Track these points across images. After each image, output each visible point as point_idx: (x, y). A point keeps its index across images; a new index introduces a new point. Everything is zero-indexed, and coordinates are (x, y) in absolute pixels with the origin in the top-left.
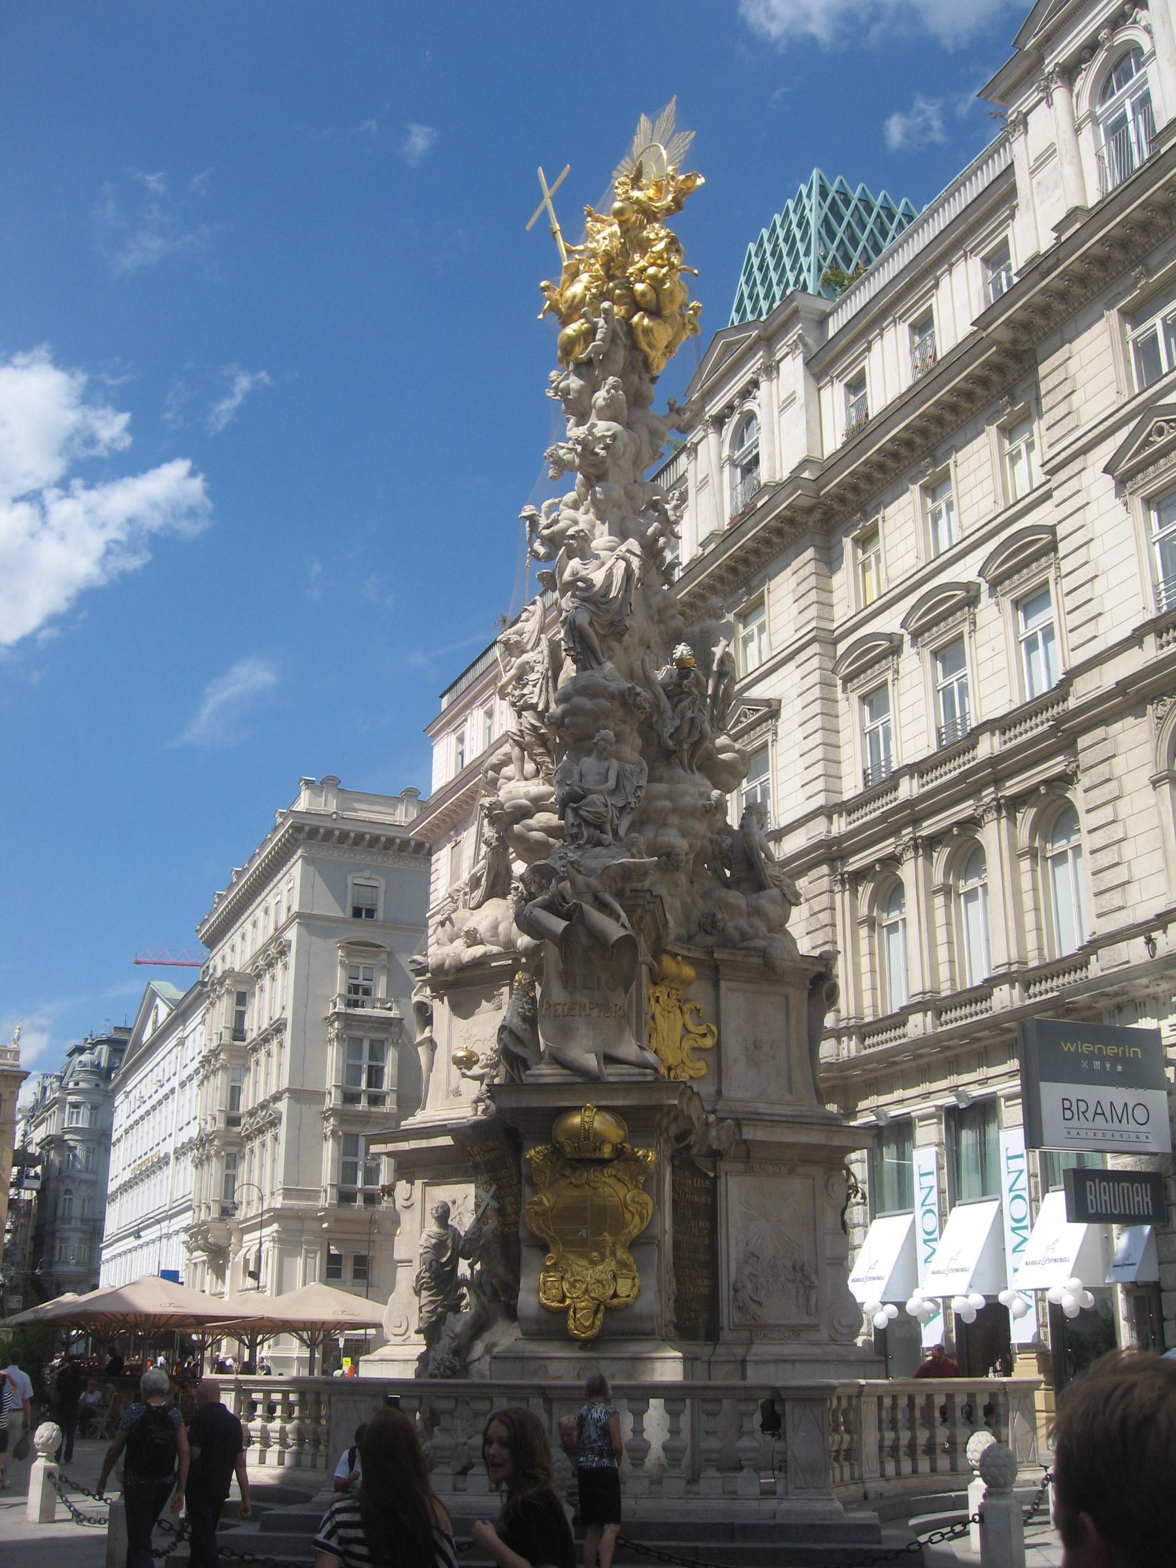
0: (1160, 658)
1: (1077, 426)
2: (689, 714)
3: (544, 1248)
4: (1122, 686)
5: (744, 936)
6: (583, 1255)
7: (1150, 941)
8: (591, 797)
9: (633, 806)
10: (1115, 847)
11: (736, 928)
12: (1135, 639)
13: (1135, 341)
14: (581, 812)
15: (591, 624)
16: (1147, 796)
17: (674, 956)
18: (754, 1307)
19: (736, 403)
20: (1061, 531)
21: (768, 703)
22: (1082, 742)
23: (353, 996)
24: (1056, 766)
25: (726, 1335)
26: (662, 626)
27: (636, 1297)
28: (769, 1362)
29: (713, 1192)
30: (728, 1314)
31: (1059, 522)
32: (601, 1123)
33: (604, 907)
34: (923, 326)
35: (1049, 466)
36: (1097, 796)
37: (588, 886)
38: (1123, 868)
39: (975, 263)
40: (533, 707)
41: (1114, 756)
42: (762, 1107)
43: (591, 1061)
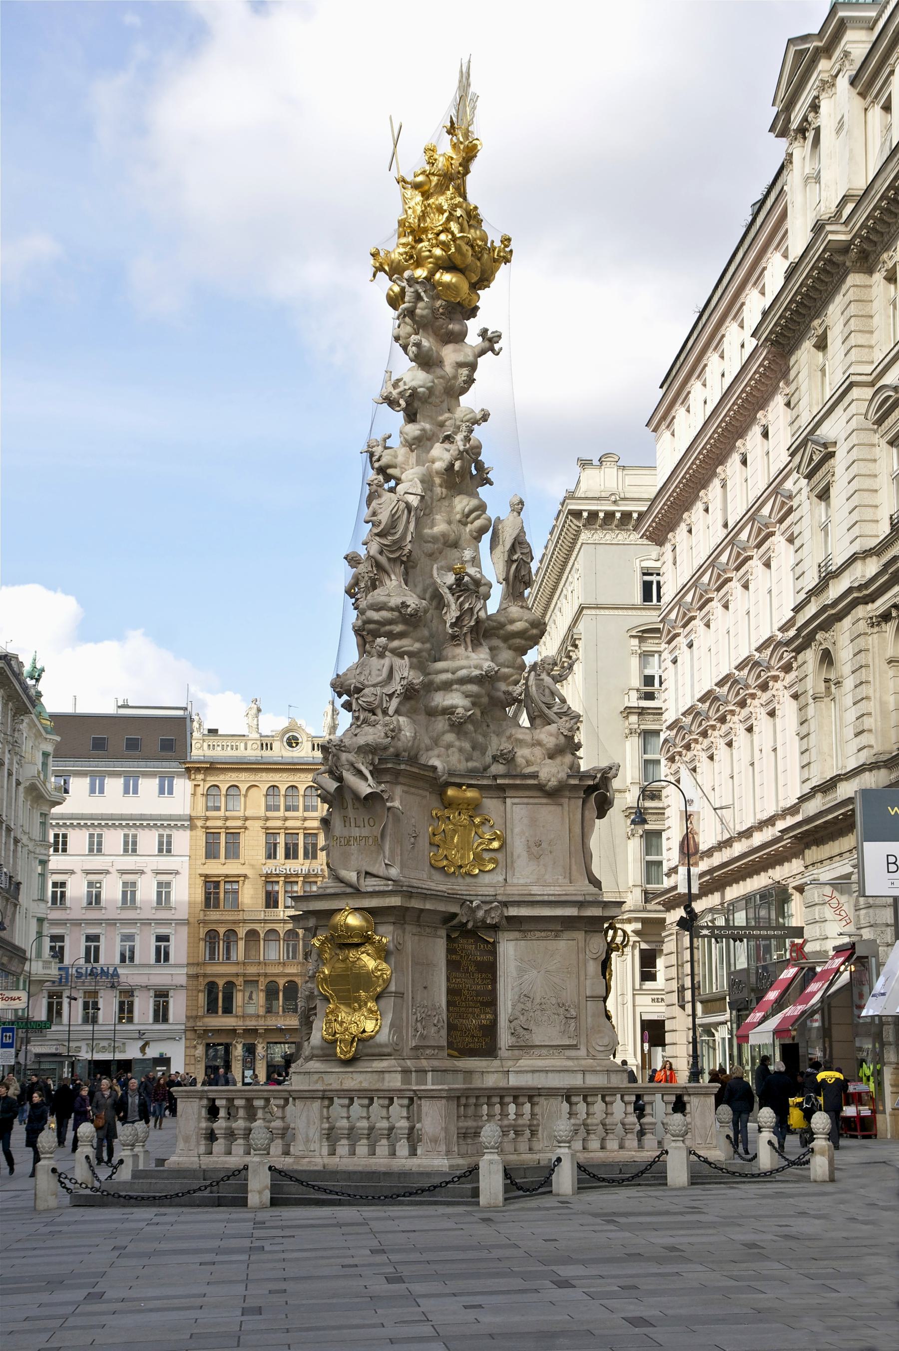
2: (466, 606)
3: (327, 999)
5: (529, 763)
6: (349, 1005)
8: (366, 691)
11: (523, 757)
14: (360, 702)
15: (381, 553)
17: (459, 786)
18: (525, 1032)
21: (825, 445)
23: (649, 689)
25: (503, 1053)
26: (469, 527)
27: (377, 1032)
28: (527, 1072)
29: (494, 952)
30: (504, 1039)
32: (354, 921)
33: (360, 773)
37: (347, 761)
42: (535, 890)
43: (352, 876)
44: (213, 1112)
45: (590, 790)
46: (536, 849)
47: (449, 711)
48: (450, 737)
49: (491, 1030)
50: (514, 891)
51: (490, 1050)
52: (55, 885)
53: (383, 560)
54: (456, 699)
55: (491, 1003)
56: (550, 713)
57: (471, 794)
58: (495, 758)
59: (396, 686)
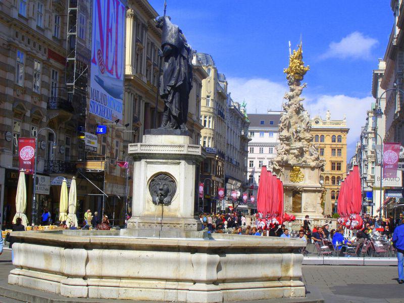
30: (303, 210)
44: (252, 220)
45: (320, 167)
46: (310, 178)
47: (294, 154)
48: (295, 158)
49: (300, 208)
50: (305, 185)
51: (300, 212)
52: (250, 162)
53: (283, 127)
54: (295, 151)
55: (301, 204)
56: (313, 154)
57: (298, 168)
58: (303, 162)
59: (284, 150)
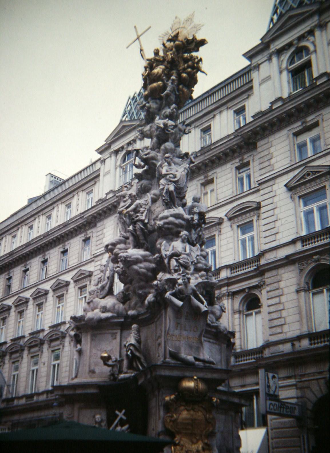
0: (303, 250)
1: (273, 170)
4: (287, 257)
7: (293, 345)
9: (195, 262)
10: (279, 312)
12: (293, 242)
13: (298, 144)
14: (181, 261)
16: (294, 296)
19: (125, 147)
20: (263, 204)
22: (267, 275)
24: (254, 282)
31: (262, 201)
34: (207, 130)
35: (260, 182)
36: (272, 294)
38: (283, 319)
39: (231, 112)
40: (142, 221)
41: (281, 281)
